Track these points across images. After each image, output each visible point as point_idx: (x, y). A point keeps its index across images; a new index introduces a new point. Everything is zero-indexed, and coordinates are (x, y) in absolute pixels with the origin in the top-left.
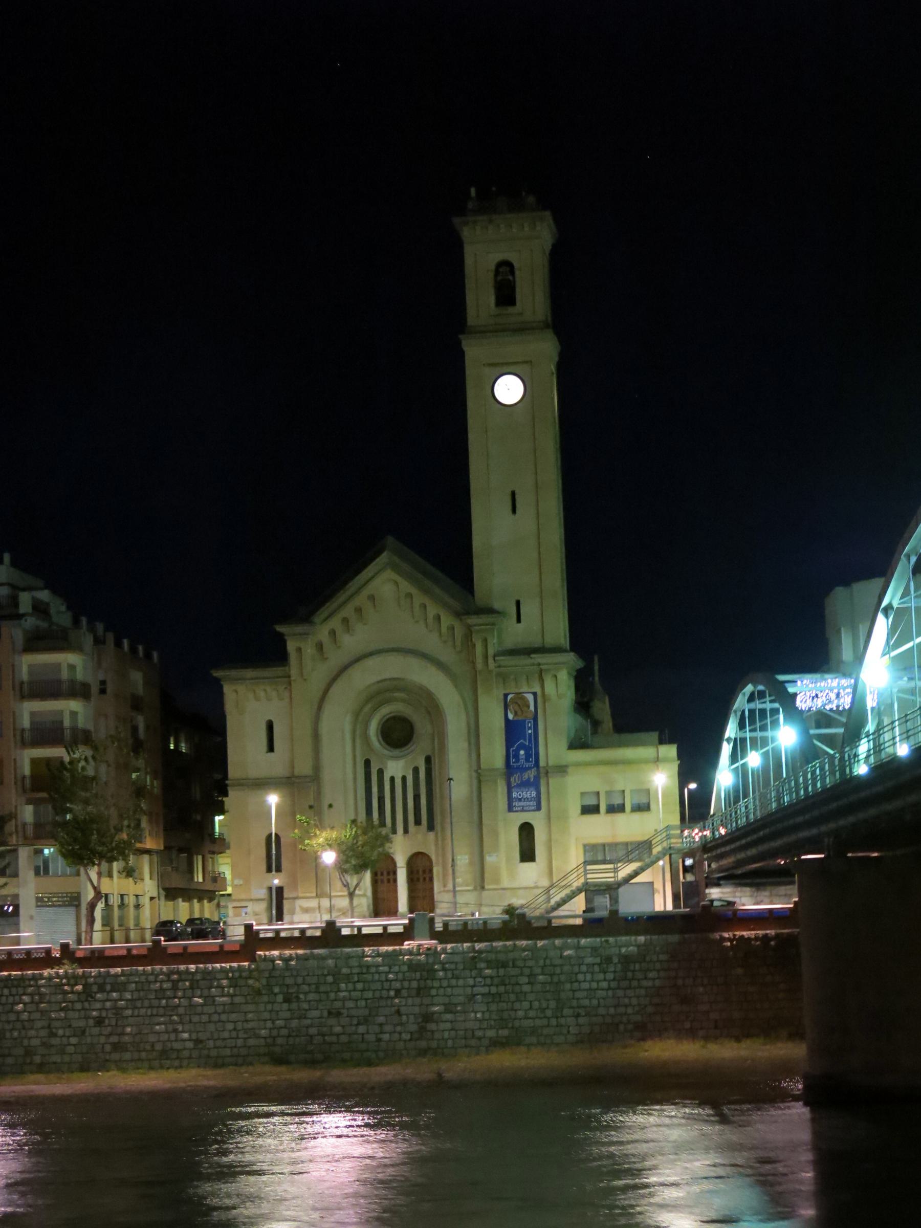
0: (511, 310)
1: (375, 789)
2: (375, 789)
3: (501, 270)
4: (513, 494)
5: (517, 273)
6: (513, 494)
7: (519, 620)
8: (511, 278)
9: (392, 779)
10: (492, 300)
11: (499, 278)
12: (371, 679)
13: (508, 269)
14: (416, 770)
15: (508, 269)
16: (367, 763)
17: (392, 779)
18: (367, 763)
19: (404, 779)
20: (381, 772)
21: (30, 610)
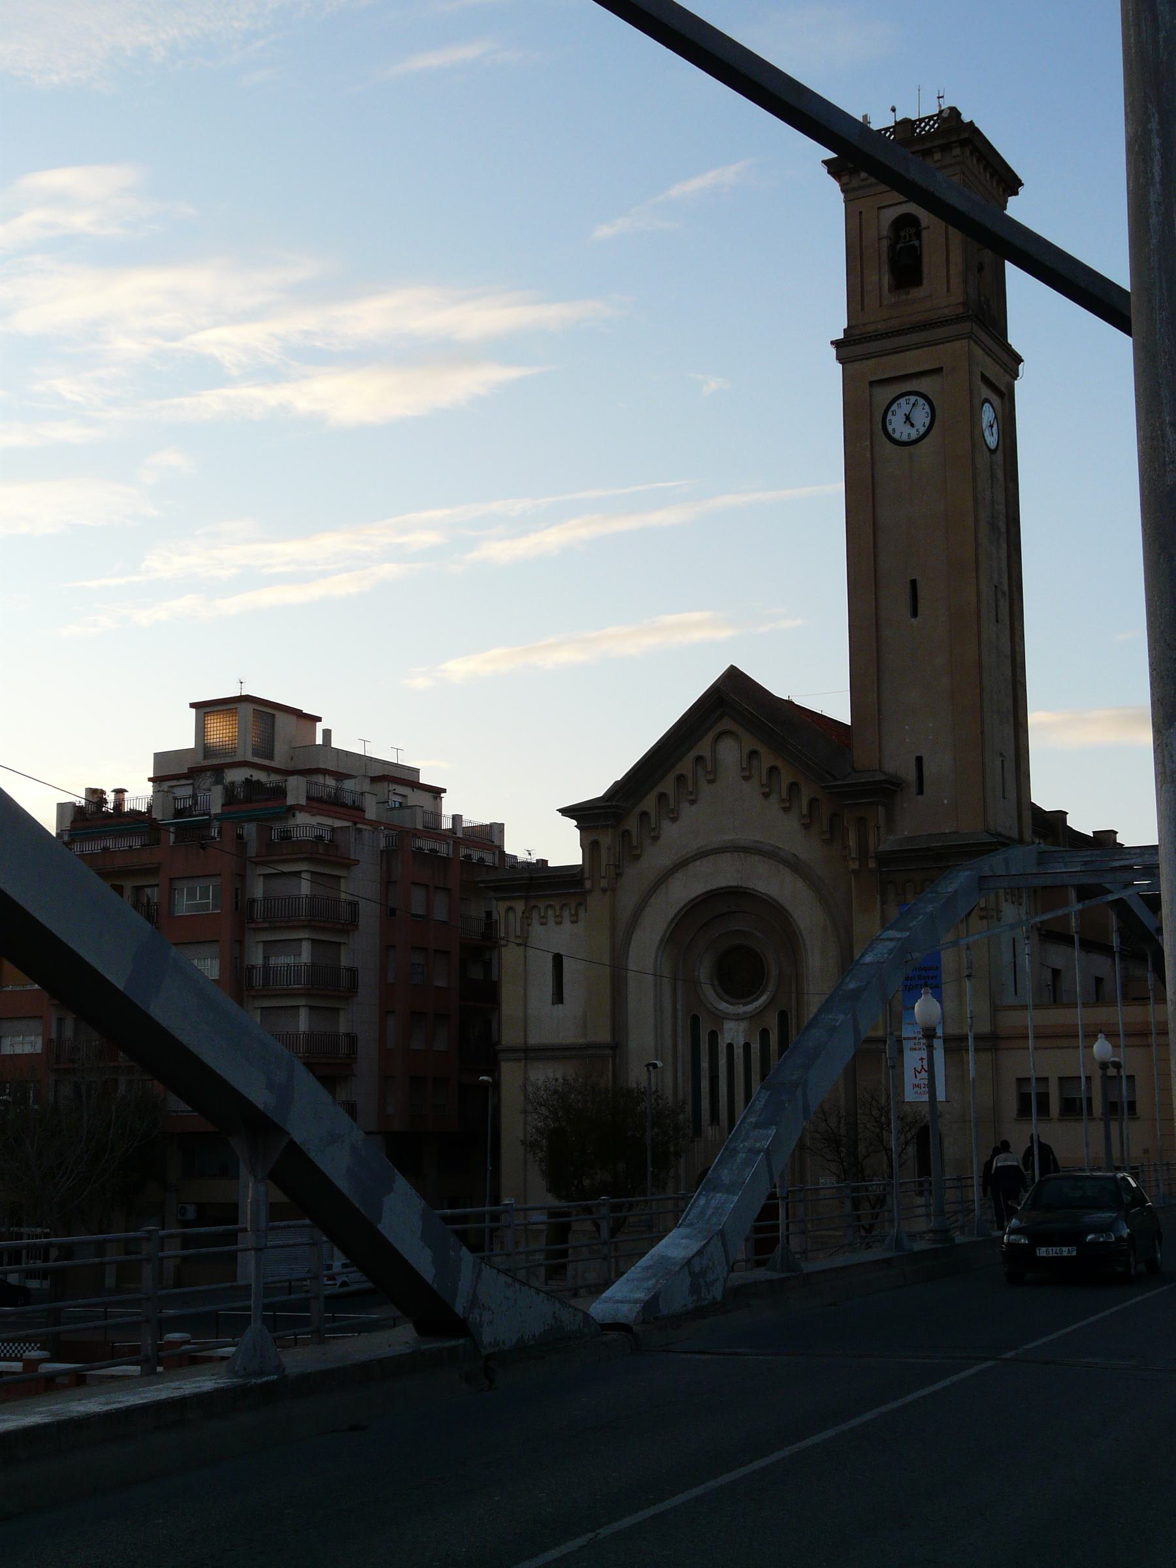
0: (916, 293)
1: (705, 1065)
2: (705, 1065)
3: (903, 234)
4: (914, 583)
5: (925, 233)
6: (914, 583)
7: (921, 791)
8: (916, 243)
9: (730, 1047)
10: (886, 279)
11: (898, 247)
12: (698, 888)
13: (913, 231)
14: (765, 1034)
15: (913, 231)
16: (695, 1020)
17: (730, 1047)
18: (695, 1020)
19: (747, 1046)
20: (714, 1036)
21: (303, 802)
